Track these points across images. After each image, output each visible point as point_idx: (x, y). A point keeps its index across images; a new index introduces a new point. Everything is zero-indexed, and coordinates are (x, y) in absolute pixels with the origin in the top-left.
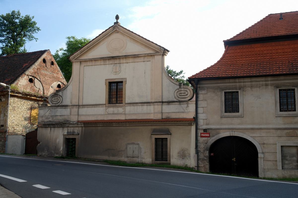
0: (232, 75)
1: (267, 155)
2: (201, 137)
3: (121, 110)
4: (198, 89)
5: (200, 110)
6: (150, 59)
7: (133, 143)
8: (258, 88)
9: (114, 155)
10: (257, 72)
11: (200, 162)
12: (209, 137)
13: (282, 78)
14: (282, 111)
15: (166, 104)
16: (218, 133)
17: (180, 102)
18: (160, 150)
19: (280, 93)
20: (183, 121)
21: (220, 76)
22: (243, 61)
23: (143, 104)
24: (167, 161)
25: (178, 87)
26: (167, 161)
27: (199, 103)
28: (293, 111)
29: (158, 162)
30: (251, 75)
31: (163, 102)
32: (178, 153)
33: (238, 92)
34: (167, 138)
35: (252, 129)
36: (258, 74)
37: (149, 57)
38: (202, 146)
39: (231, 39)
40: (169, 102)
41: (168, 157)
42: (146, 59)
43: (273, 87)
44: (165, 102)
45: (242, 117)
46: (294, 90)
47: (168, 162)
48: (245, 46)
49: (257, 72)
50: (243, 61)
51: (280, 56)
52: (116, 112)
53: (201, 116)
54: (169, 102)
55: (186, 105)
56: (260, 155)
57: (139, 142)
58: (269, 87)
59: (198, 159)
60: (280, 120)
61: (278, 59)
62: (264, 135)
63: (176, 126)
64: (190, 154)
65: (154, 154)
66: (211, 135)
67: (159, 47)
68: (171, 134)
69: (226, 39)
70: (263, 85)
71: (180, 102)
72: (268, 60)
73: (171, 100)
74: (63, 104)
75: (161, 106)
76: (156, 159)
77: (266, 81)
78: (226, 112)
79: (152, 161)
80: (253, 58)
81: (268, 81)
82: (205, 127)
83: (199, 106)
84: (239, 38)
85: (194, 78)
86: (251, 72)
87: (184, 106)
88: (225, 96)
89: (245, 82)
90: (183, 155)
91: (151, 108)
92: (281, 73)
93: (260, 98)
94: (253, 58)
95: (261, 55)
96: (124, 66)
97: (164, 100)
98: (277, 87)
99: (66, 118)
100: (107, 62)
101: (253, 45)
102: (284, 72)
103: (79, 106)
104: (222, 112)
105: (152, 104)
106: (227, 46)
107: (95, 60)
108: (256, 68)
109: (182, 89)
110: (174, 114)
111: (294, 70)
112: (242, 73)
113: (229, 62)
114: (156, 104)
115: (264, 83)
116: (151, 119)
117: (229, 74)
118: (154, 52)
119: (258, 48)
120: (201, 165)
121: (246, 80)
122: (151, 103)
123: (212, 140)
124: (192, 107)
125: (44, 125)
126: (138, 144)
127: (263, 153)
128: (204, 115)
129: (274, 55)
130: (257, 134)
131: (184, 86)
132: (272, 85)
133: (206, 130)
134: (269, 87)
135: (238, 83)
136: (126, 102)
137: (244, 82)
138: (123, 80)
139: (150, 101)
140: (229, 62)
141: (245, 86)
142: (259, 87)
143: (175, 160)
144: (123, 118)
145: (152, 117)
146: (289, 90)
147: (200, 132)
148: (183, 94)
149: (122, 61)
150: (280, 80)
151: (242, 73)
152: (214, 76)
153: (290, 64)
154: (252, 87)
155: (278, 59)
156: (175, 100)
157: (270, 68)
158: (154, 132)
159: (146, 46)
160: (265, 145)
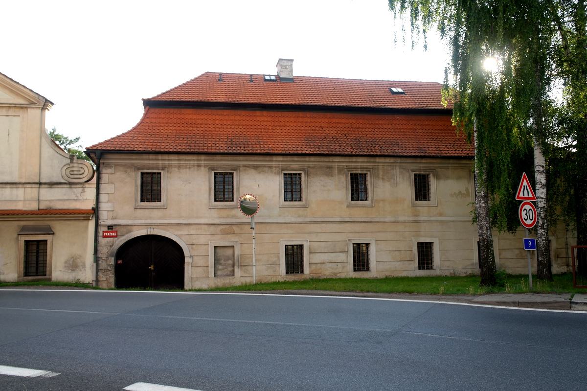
0: (153, 150)
1: (196, 259)
2: (104, 237)
4: (101, 166)
5: (103, 197)
6: (18, 112)
8: (188, 170)
10: (188, 147)
11: (100, 274)
12: (116, 237)
13: (219, 157)
14: (217, 201)
15: (46, 186)
16: (130, 231)
17: (70, 184)
18: (34, 259)
19: (215, 177)
20: (75, 214)
21: (136, 149)
22: (170, 131)
23: (4, 186)
24: (46, 275)
25: (68, 161)
26: (46, 275)
27: (102, 186)
28: (230, 201)
29: (30, 278)
30: (179, 150)
31: (40, 184)
32: (66, 262)
33: (160, 173)
34: (46, 241)
35: (178, 225)
36: (188, 150)
37: (17, 110)
38: (104, 251)
39: (154, 98)
40: (52, 184)
41: (48, 269)
42: (11, 112)
43: (207, 169)
44: (45, 184)
45: (164, 208)
46: (232, 174)
47: (47, 277)
48: (172, 110)
49: (188, 147)
50: (170, 131)
51: (217, 130)
53: (104, 207)
54: (52, 184)
55: (80, 190)
56: (187, 260)
58: (203, 168)
59: (98, 270)
60: (214, 213)
61: (214, 132)
62: (193, 232)
63: (62, 222)
64: (84, 264)
65: (22, 266)
66: (119, 234)
67: (37, 96)
68: (53, 234)
69: (146, 98)
70: (194, 166)
71: (70, 184)
72: (202, 132)
73: (55, 180)
75: (38, 189)
76: (27, 273)
77: (198, 160)
78: (142, 201)
79: (19, 277)
80: (183, 128)
81: (201, 160)
82: (110, 222)
83: (102, 191)
84: (165, 98)
85: (95, 150)
86: (179, 147)
87: (77, 190)
88: (142, 178)
89: (171, 160)
90: (73, 264)
91: (19, 193)
92: (217, 151)
93: (190, 183)
94: (183, 128)
95: (194, 125)
97: (43, 181)
98: (212, 169)
101: (183, 111)
102: (221, 151)
104: (136, 200)
105: (20, 186)
106: (147, 107)
108: (185, 142)
109: (75, 165)
110: (61, 202)
111: (234, 148)
112: (167, 147)
113: (149, 131)
114: (28, 186)
115: (196, 162)
116: (19, 210)
117: (149, 147)
118: (27, 103)
119: (189, 114)
120: (102, 277)
121: (173, 157)
122: (20, 183)
124: (90, 192)
127: (191, 257)
128: (110, 204)
129: (209, 126)
130: (184, 231)
131: (79, 160)
132: (205, 166)
133: (112, 226)
134: (203, 168)
135: (161, 161)
137: (169, 160)
139: (17, 180)
140: (149, 131)
141: (170, 166)
142: (190, 168)
145: (20, 207)
146: (227, 174)
147: (101, 230)
148: (75, 173)
150: (216, 160)
151: (167, 147)
152: (126, 149)
153: (229, 140)
154: (179, 167)
155: (214, 132)
156: (63, 181)
157: (203, 144)
158: (23, 231)
159: (12, 91)
160: (194, 246)
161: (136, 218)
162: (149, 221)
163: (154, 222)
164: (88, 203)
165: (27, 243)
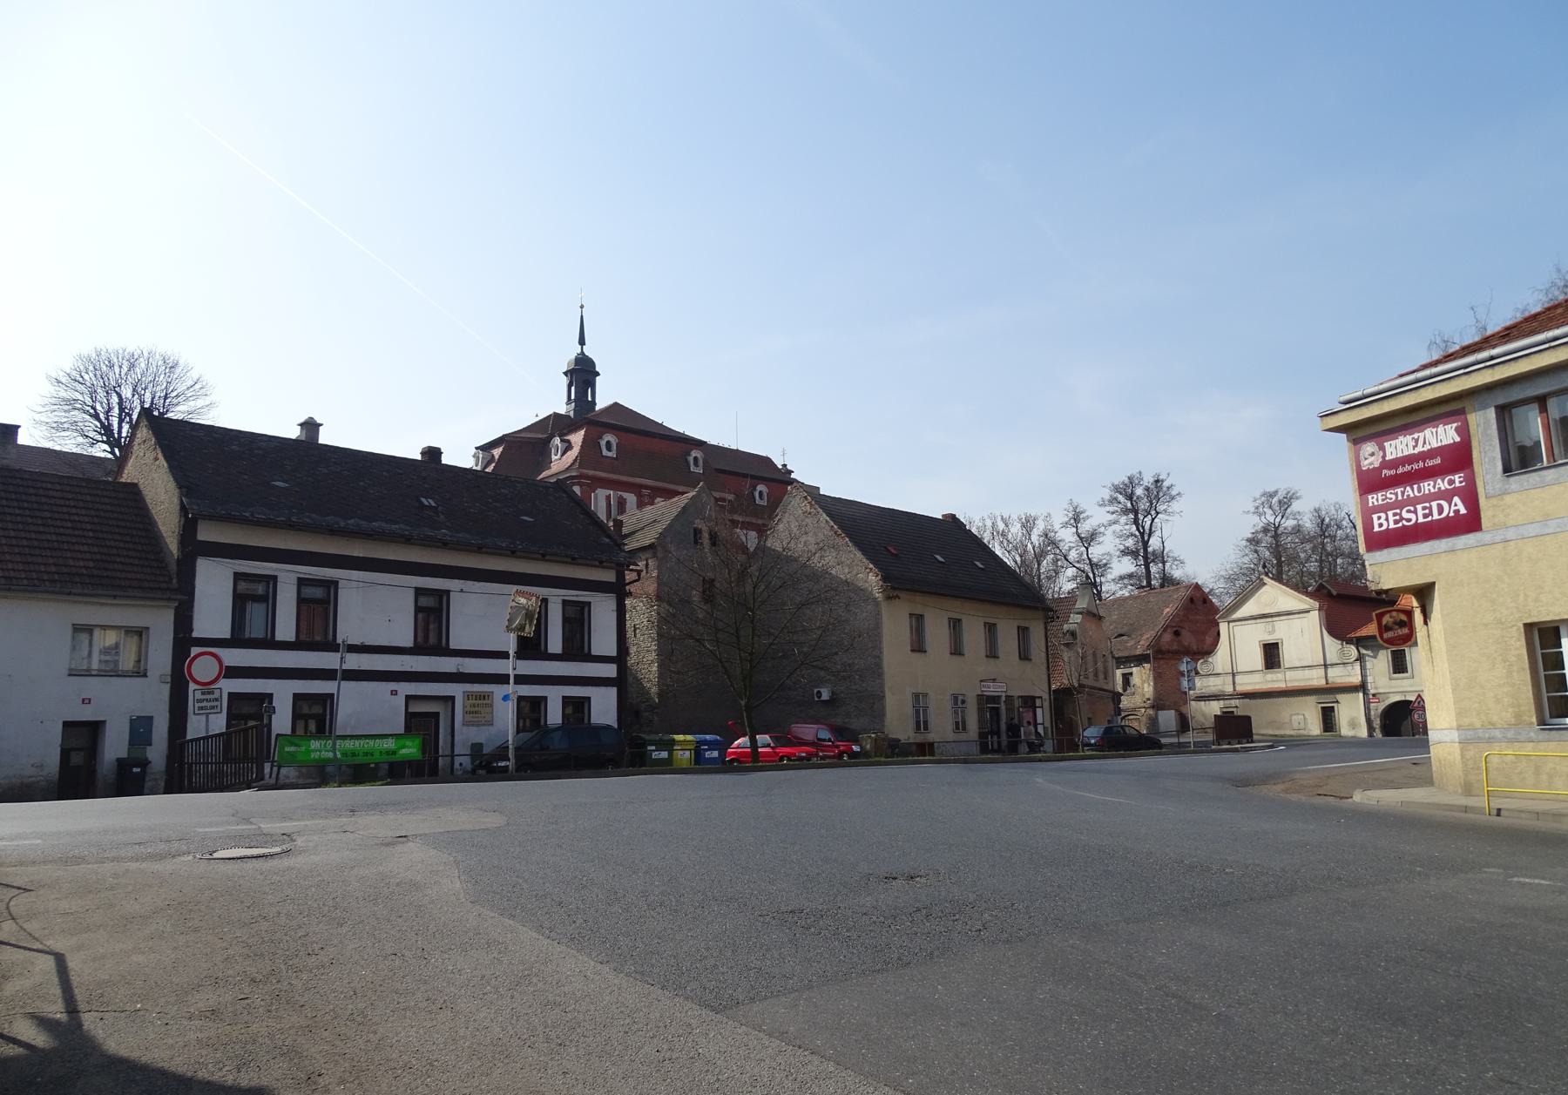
7: (1298, 714)
9: (1278, 728)
16: (1388, 698)
25: (1340, 646)
32: (1349, 722)
52: (1275, 679)
53: (1370, 679)
57: (1304, 712)
71: (1344, 664)
74: (1214, 672)
87: (1349, 668)
90: (1353, 724)
99: (1220, 687)
100: (1258, 621)
103: (1234, 675)
104: (1389, 673)
123: (1382, 706)
125: (1197, 697)
138: (1279, 641)
143: (1345, 730)
144: (1282, 686)
161: (1391, 687)
162: (1401, 690)
163: (1405, 689)
164: (1356, 679)
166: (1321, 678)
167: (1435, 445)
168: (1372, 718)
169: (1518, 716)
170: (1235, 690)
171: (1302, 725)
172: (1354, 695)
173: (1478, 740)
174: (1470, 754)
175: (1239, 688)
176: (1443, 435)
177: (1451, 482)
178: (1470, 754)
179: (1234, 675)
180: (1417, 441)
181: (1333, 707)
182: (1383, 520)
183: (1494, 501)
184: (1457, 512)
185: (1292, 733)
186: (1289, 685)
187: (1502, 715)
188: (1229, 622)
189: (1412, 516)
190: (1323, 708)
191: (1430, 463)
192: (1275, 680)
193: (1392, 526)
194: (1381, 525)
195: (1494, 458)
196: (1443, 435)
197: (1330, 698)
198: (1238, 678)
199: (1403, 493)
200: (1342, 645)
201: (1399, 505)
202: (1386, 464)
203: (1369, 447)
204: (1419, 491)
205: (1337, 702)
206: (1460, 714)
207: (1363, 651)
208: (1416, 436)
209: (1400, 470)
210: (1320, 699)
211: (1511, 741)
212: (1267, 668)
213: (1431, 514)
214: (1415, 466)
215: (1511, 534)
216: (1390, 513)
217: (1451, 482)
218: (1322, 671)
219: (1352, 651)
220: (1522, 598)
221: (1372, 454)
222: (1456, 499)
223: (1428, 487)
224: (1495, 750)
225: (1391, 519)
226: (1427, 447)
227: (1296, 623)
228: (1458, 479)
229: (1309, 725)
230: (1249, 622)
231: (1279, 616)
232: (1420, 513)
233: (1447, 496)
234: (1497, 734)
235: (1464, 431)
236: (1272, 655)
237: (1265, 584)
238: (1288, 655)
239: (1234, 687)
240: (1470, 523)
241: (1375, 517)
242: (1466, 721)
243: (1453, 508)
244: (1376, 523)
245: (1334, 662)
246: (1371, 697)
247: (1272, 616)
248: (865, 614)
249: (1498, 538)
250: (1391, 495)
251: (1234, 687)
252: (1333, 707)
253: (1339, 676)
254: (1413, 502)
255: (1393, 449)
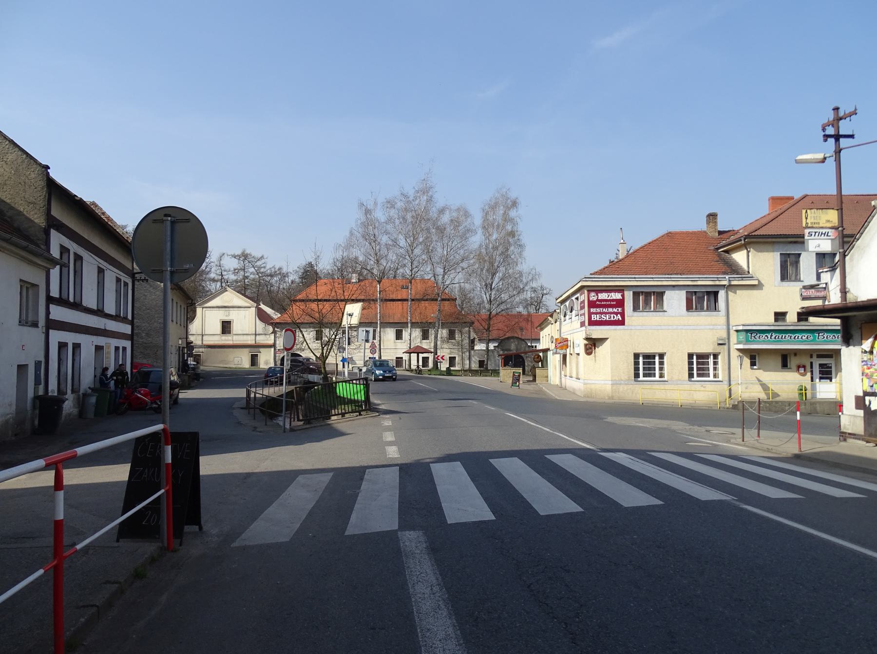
3: (230, 338)
9: (226, 364)
32: (265, 362)
71: (265, 334)
87: (268, 336)
96: (231, 312)
100: (221, 309)
103: (203, 335)
107: (213, 307)
126: (241, 358)
136: (234, 333)
138: (231, 321)
144: (231, 343)
149: (230, 309)
164: (271, 342)
165: (252, 355)
166: (253, 340)
167: (614, 298)
168: (277, 360)
169: (629, 377)
170: (202, 343)
171: (240, 363)
172: (269, 349)
173: (617, 384)
174: (614, 388)
175: (204, 343)
176: (618, 296)
177: (618, 310)
178: (614, 388)
179: (203, 335)
180: (609, 296)
181: (257, 355)
182: (595, 317)
183: (629, 318)
184: (619, 319)
185: (234, 366)
186: (235, 342)
187: (624, 377)
188: (203, 308)
189: (605, 318)
190: (252, 355)
191: (612, 303)
192: (227, 340)
193: (598, 319)
194: (594, 318)
195: (630, 306)
196: (618, 296)
197: (256, 350)
198: (204, 337)
199: (602, 310)
200: (266, 325)
201: (600, 313)
202: (598, 300)
203: (593, 294)
204: (608, 310)
205: (260, 352)
206: (612, 376)
207: (276, 329)
208: (609, 294)
209: (603, 303)
210: (251, 350)
211: (626, 384)
212: (222, 334)
213: (611, 318)
214: (607, 303)
215: (633, 328)
216: (598, 315)
217: (618, 310)
218: (253, 337)
219: (271, 329)
220: (634, 346)
221: (594, 296)
222: (619, 315)
223: (610, 310)
224: (622, 386)
225: (598, 317)
226: (612, 298)
227: (242, 312)
228: (620, 310)
229: (244, 363)
230: (215, 309)
231: (233, 308)
232: (607, 317)
233: (617, 314)
234: (622, 382)
235: (623, 296)
236: (226, 327)
237: (227, 291)
238: (236, 328)
239: (202, 342)
240: (622, 323)
241: (593, 315)
242: (614, 378)
243: (618, 318)
244: (593, 317)
245: (260, 333)
246: (277, 350)
247: (229, 308)
248: (153, 297)
249: (629, 328)
250: (598, 310)
251: (202, 342)
252: (257, 355)
253: (261, 340)
254: (606, 313)
255: (601, 296)
